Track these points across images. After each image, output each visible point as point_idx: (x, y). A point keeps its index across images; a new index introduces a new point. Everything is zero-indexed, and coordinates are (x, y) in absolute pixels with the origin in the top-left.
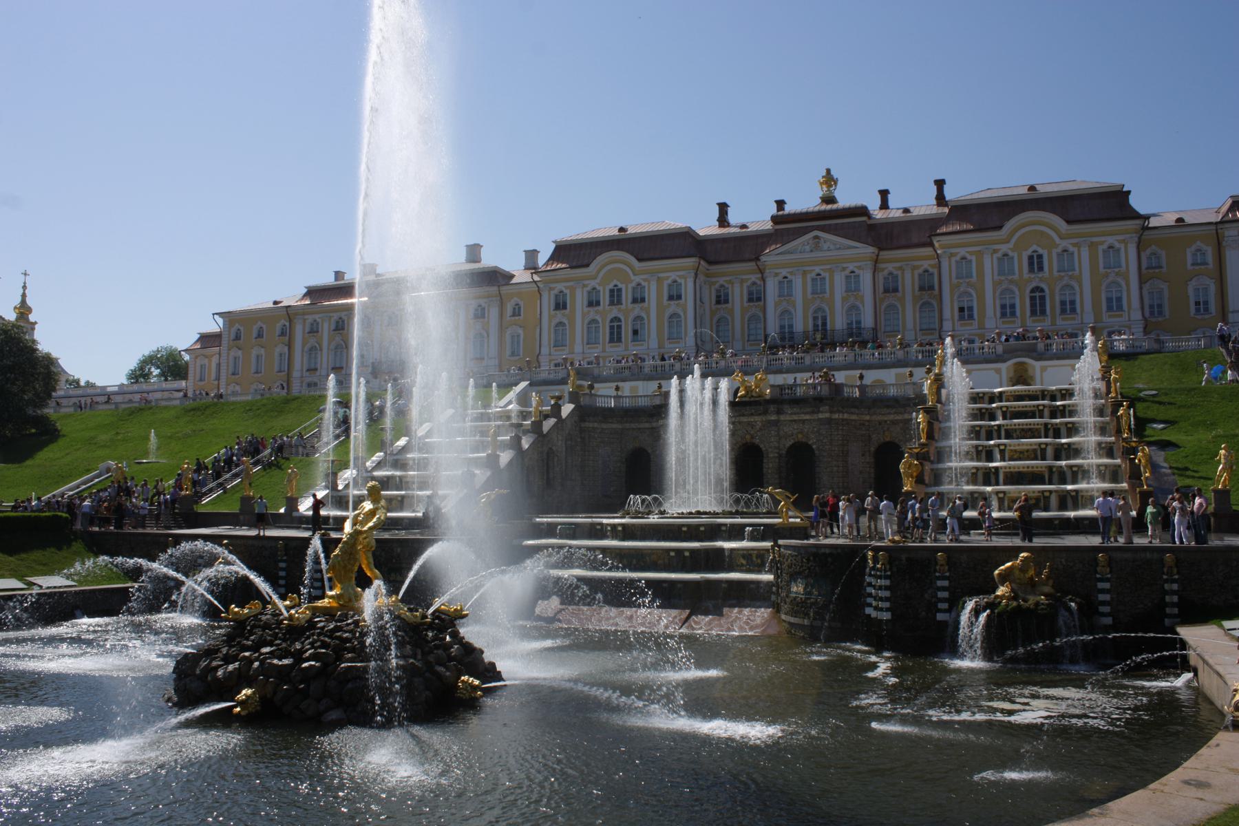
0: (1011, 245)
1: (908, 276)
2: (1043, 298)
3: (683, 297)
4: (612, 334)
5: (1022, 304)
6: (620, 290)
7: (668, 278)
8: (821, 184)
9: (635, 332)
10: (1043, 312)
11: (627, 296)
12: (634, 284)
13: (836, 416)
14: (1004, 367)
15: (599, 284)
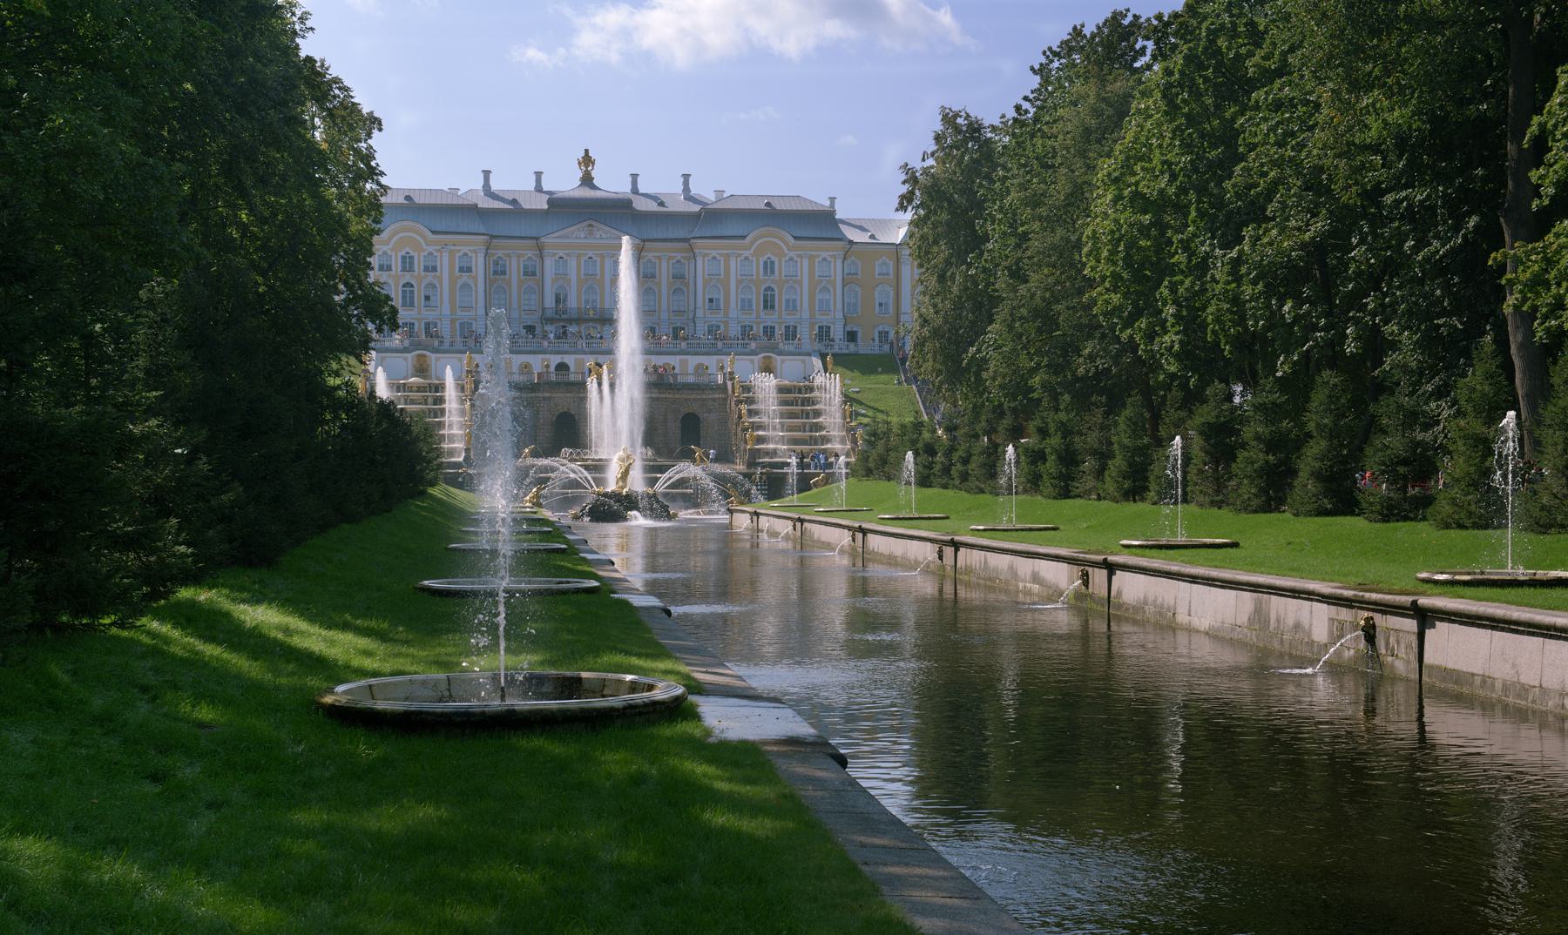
0: (752, 251)
1: (664, 265)
2: (773, 296)
3: (474, 270)
4: (404, 297)
5: (757, 300)
6: (412, 258)
7: (459, 251)
8: (579, 163)
9: (427, 298)
10: (773, 307)
11: (418, 266)
12: (426, 253)
13: (663, 396)
14: (755, 358)
15: (391, 251)
